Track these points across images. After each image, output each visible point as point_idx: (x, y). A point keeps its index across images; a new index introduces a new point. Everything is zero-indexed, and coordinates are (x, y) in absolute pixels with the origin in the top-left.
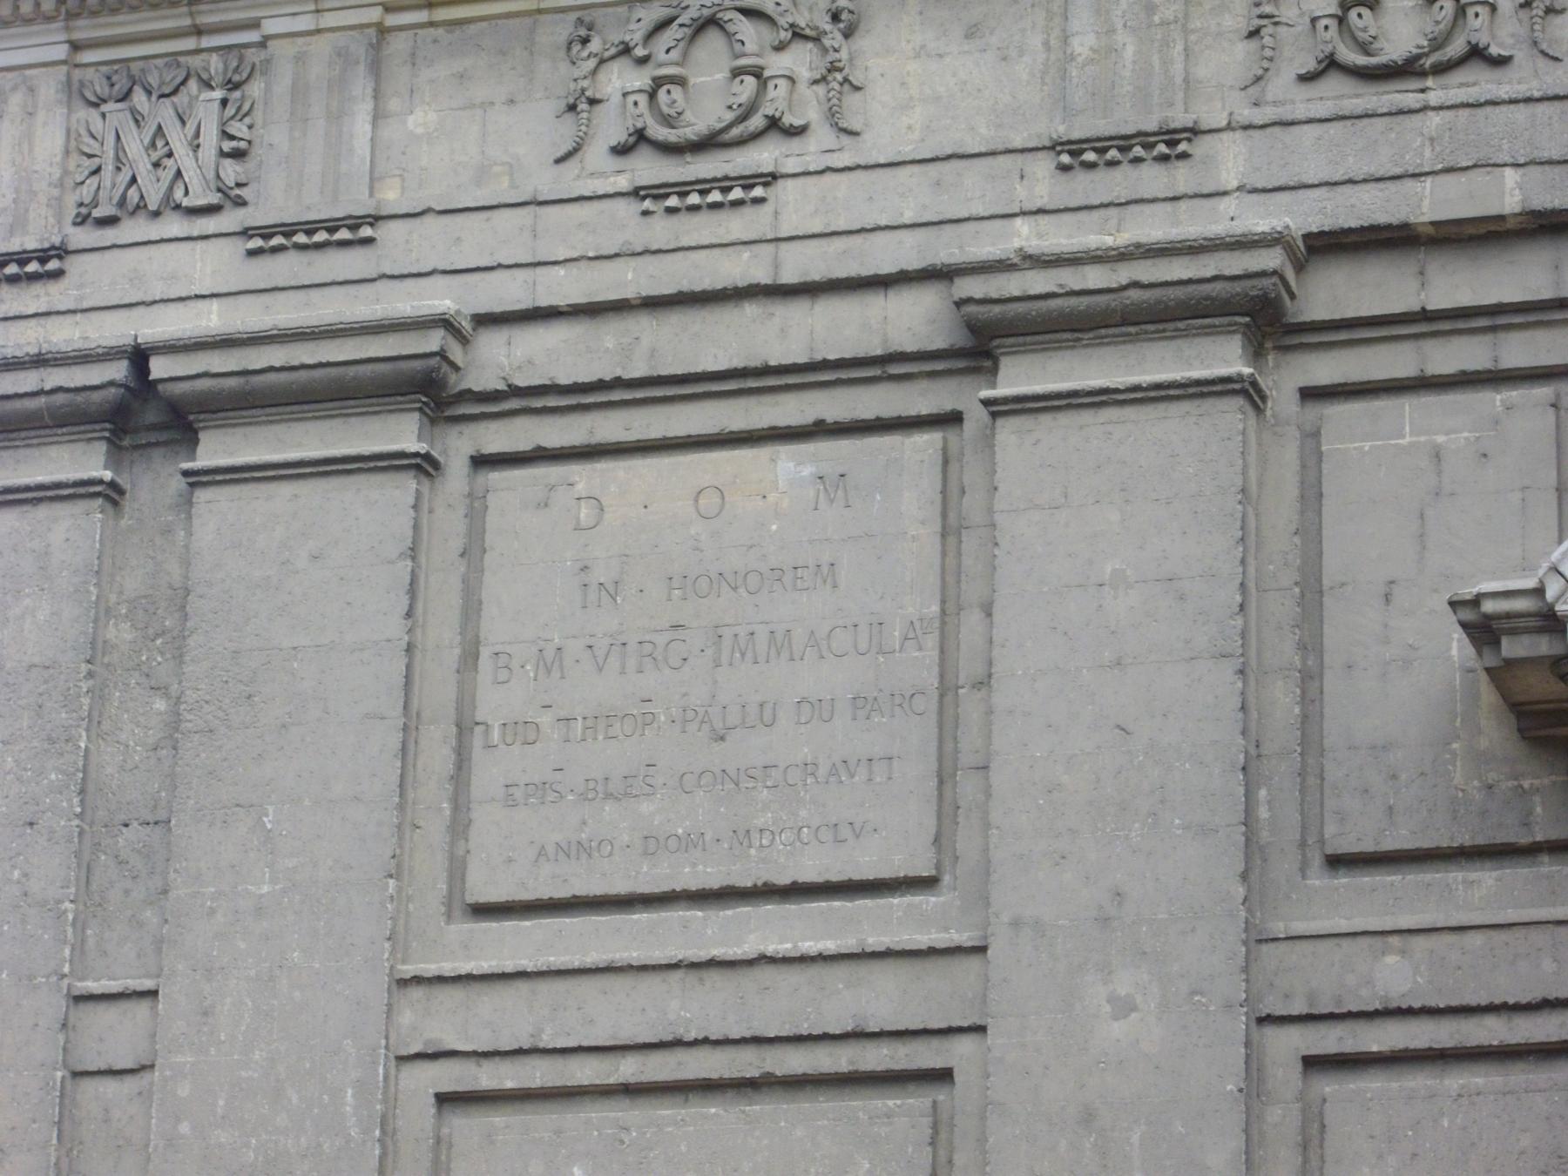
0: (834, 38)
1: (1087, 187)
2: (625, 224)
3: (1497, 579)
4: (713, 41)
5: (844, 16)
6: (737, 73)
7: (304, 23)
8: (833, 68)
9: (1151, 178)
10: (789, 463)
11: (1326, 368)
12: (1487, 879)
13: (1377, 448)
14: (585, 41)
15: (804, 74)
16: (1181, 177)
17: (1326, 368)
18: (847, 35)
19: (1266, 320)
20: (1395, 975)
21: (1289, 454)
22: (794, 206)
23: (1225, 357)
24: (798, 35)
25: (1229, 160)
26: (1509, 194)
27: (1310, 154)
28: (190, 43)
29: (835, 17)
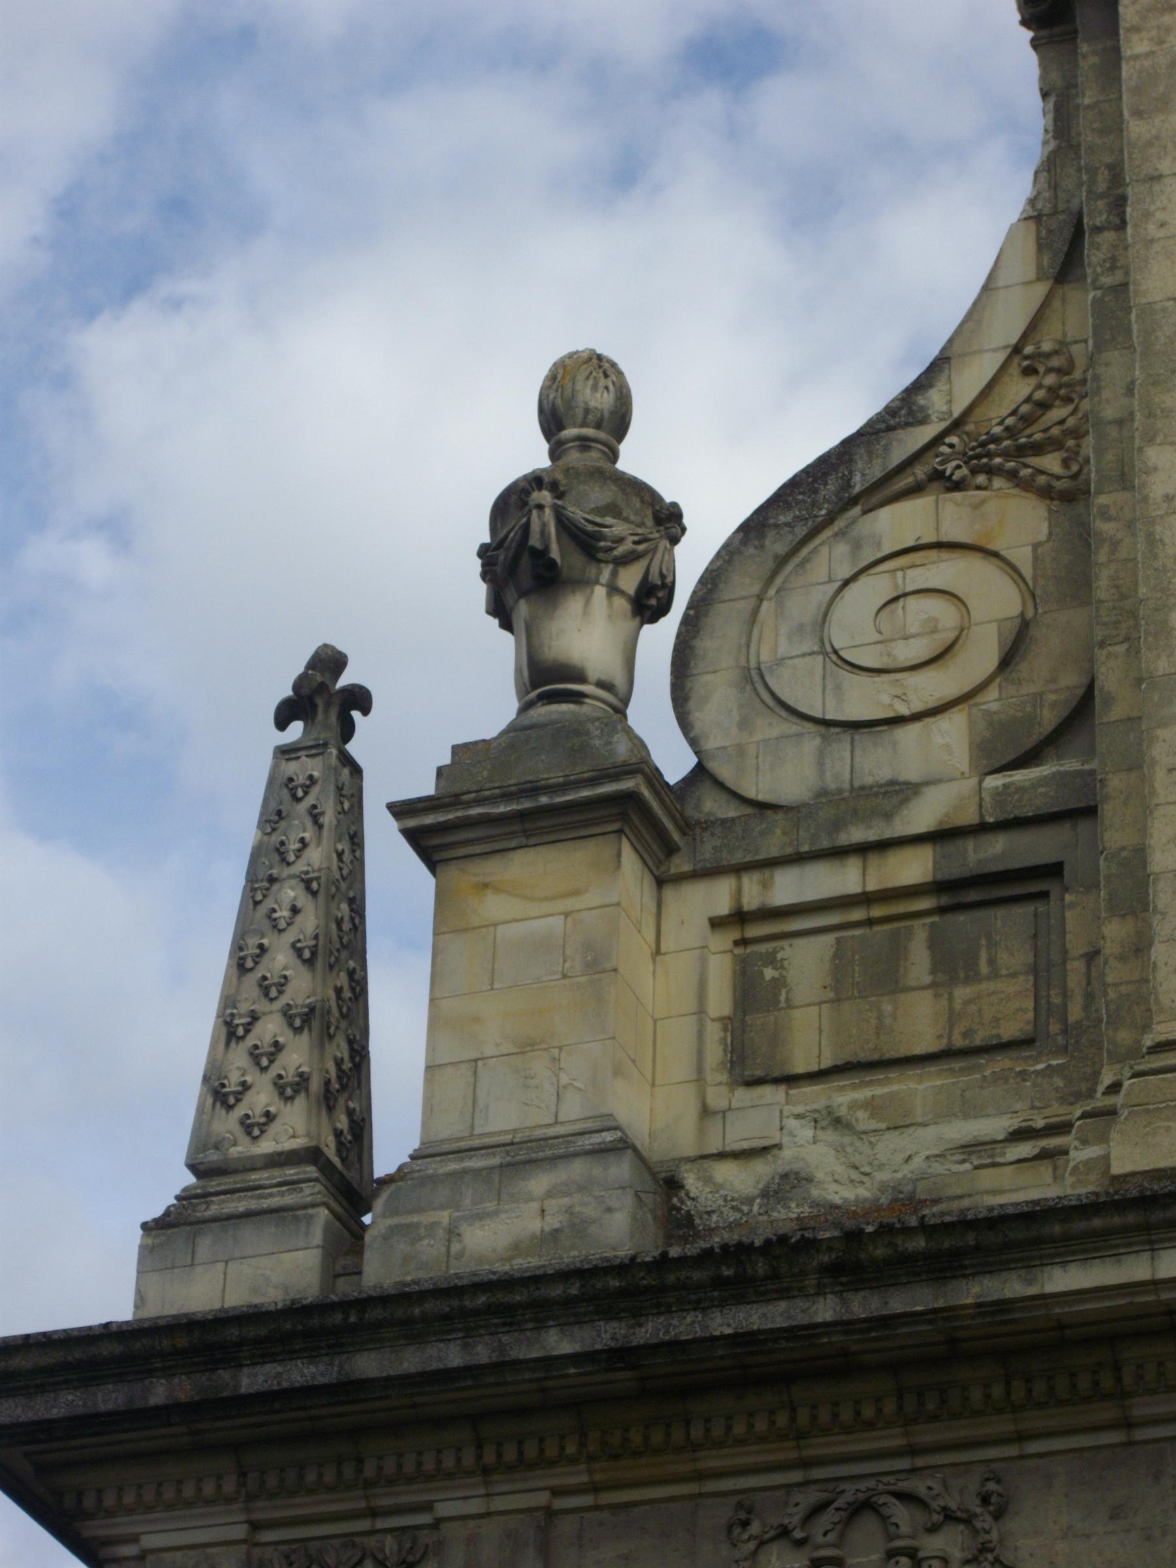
0: (985, 1521)
4: (868, 1525)
5: (994, 1499)
6: (891, 1554)
7: (475, 1506)
8: (984, 1549)
14: (745, 1524)
15: (957, 1554)
18: (998, 1516)
24: (949, 1517)
28: (363, 1525)
29: (985, 1500)
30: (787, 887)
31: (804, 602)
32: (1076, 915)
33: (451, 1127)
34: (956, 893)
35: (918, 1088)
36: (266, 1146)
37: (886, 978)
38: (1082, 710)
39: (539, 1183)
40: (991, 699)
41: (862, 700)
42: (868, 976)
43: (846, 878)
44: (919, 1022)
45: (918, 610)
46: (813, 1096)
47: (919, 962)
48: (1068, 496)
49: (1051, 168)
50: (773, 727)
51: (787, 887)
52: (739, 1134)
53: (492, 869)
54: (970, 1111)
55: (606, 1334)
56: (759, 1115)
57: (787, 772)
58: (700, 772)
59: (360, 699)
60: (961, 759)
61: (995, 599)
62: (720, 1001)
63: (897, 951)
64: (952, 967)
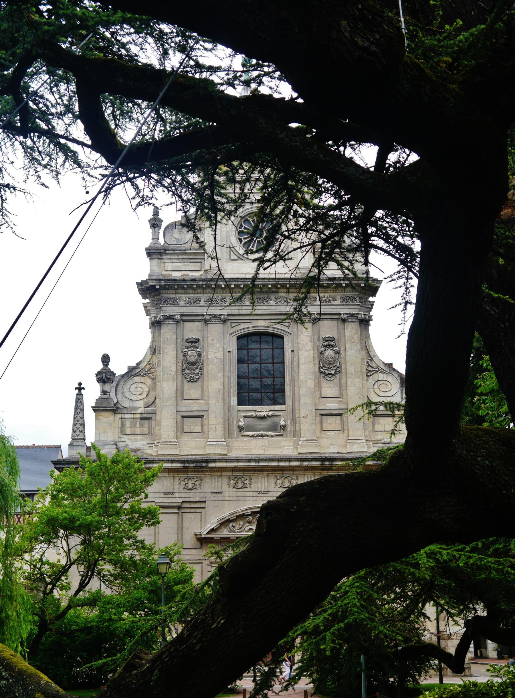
1: (166, 496)
3: (198, 532)
9: (171, 496)
11: (183, 511)
12: (194, 550)
13: (187, 517)
16: (173, 496)
17: (183, 511)
19: (179, 508)
20: (188, 557)
21: (180, 517)
23: (176, 511)
25: (177, 495)
26: (197, 499)
27: (183, 495)
30: (127, 416)
31: (128, 386)
32: (153, 423)
33: (98, 439)
34: (142, 419)
35: (139, 437)
36: (79, 438)
37: (135, 426)
39: (107, 447)
40: (145, 400)
41: (134, 398)
42: (133, 426)
43: (132, 416)
44: (138, 431)
46: (128, 437)
49: (152, 342)
50: (124, 399)
51: (127, 416)
52: (122, 440)
53: (100, 413)
54: (142, 440)
56: (124, 438)
57: (126, 404)
58: (118, 402)
59: (83, 388)
60: (142, 406)
61: (146, 390)
62: (120, 426)
63: (136, 423)
64: (141, 426)
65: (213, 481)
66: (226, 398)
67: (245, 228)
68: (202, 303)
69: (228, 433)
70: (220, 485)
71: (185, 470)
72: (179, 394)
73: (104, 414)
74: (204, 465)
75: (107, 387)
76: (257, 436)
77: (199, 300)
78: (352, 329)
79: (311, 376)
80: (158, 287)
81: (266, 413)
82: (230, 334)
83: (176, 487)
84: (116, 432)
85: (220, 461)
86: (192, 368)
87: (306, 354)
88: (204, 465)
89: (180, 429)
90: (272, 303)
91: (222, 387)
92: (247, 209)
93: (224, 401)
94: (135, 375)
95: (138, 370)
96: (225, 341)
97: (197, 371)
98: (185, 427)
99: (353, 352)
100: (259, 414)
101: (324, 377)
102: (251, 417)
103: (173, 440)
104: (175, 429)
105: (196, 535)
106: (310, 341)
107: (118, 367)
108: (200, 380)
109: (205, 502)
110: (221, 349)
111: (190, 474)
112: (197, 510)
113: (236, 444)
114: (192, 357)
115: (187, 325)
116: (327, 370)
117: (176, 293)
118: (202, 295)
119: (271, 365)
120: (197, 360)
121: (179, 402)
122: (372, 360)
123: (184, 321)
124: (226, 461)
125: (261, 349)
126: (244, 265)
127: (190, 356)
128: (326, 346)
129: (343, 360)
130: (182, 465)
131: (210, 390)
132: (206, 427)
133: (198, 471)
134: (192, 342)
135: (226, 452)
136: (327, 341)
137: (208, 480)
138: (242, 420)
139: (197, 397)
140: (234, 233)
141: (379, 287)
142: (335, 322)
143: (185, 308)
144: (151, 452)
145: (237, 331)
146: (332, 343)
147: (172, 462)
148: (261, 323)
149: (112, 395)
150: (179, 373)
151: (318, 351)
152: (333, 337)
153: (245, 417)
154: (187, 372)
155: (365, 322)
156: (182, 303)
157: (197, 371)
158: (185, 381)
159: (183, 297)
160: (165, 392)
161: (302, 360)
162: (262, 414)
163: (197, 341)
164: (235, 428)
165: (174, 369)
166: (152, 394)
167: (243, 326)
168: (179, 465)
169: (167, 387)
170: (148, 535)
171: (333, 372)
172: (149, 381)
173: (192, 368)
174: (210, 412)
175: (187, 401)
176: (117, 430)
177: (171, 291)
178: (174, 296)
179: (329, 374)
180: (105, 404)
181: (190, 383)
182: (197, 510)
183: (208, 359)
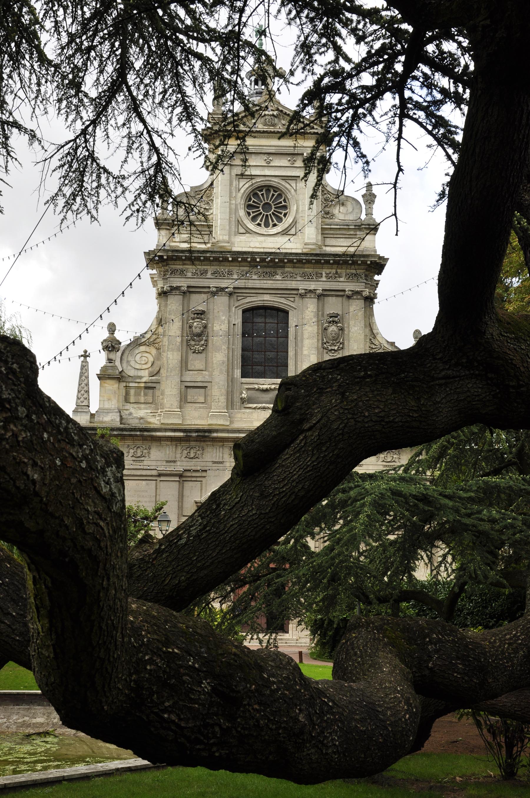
2: (132, 462)
9: (172, 464)
10: (144, 482)
11: (184, 479)
17: (184, 479)
19: (181, 476)
22: (145, 463)
25: (178, 463)
27: (185, 464)
30: (131, 385)
32: (157, 393)
33: (102, 406)
34: (146, 388)
35: (143, 406)
37: (139, 395)
38: (159, 372)
39: (111, 414)
40: (150, 369)
41: (138, 366)
42: (137, 394)
43: (136, 385)
44: (142, 399)
45: (144, 358)
46: (132, 405)
47: (142, 394)
48: (158, 349)
49: (158, 312)
50: (129, 368)
51: (131, 385)
52: (126, 408)
55: (120, 433)
57: (131, 372)
61: (151, 359)
64: (145, 395)
65: (215, 451)
66: (231, 371)
67: (254, 202)
68: (209, 275)
69: (230, 404)
70: (221, 455)
71: (186, 439)
72: (184, 364)
73: (109, 381)
74: (207, 434)
75: (112, 356)
76: (259, 408)
77: (206, 272)
78: (356, 307)
79: (315, 352)
80: (165, 257)
81: (269, 386)
82: (236, 307)
83: (178, 455)
84: (121, 401)
85: (223, 431)
86: (196, 339)
87: (310, 329)
88: (207, 434)
89: (183, 399)
90: (278, 277)
91: (226, 359)
92: (257, 182)
93: (228, 372)
94: (141, 345)
95: (143, 340)
96: (231, 314)
97: (203, 342)
98: (189, 397)
99: (356, 329)
100: (261, 387)
101: (327, 353)
102: (254, 389)
103: (176, 410)
104: (179, 399)
105: (196, 503)
106: (314, 317)
107: (124, 337)
108: (205, 352)
109: (206, 471)
110: (226, 322)
111: (193, 444)
112: (198, 479)
113: (239, 415)
114: (198, 329)
115: (194, 297)
116: (331, 346)
117: (183, 265)
118: (209, 267)
119: (275, 339)
120: (202, 332)
121: (184, 372)
122: (375, 337)
123: (191, 292)
124: (228, 431)
125: (265, 323)
126: (252, 238)
127: (196, 328)
128: (330, 322)
129: (346, 337)
130: (185, 434)
131: (215, 362)
132: (209, 398)
133: (200, 441)
134: (198, 314)
135: (228, 423)
136: (331, 317)
137: (210, 449)
138: (244, 392)
139: (202, 367)
140: (243, 206)
141: (385, 265)
142: (340, 299)
143: (192, 280)
144: (155, 421)
145: (243, 304)
146: (336, 319)
147: (175, 430)
148: (267, 297)
149: (118, 363)
150: (185, 343)
151: (322, 327)
152: (337, 314)
153: (248, 389)
154: (193, 343)
155: (370, 300)
156: (189, 275)
157: (203, 342)
158: (190, 352)
159: (190, 269)
160: (170, 362)
161: (306, 335)
162: (265, 387)
163: (203, 313)
164: (237, 400)
165: (179, 339)
166: (158, 363)
167: (248, 300)
168: (181, 434)
169: (172, 357)
170: (149, 502)
171: (336, 348)
172: (154, 351)
173: (196, 339)
174: (213, 384)
175: (191, 372)
176: (122, 398)
177: (178, 262)
178: (181, 267)
179: (332, 350)
180: (110, 372)
181: (195, 355)
182: (198, 479)
183: (213, 330)
